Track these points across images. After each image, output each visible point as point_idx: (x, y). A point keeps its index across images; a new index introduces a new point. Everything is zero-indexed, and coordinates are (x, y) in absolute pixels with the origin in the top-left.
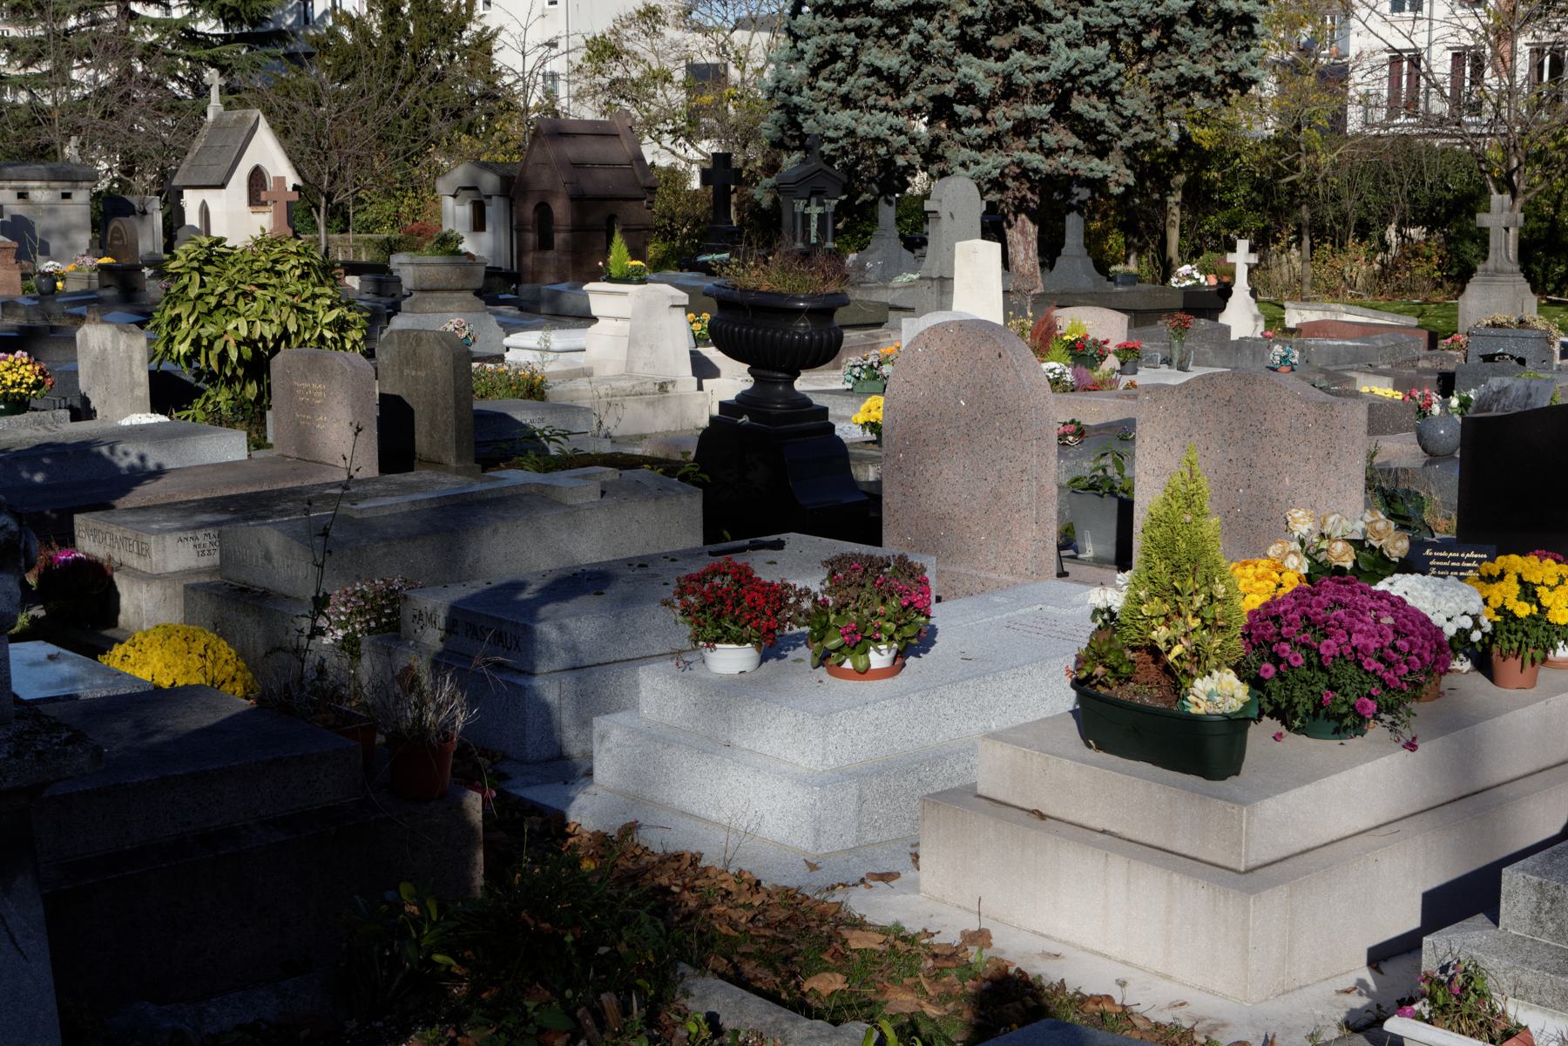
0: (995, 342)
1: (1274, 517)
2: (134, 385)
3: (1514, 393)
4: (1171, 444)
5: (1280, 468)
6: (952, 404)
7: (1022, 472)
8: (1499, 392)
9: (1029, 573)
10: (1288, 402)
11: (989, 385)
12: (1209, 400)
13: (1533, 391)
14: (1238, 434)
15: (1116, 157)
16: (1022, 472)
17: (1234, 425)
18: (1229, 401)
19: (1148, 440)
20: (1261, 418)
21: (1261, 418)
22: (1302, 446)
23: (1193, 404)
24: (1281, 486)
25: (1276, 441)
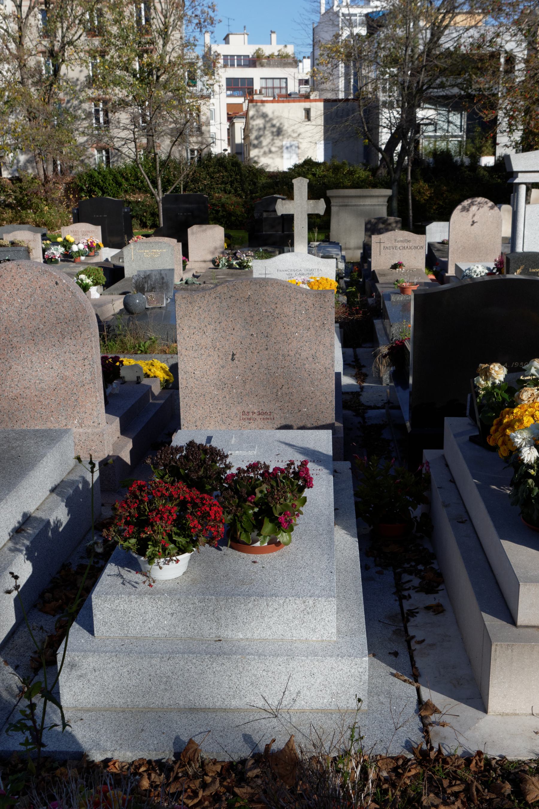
0: (51, 274)
1: (286, 365)
2: (93, 381)
3: (154, 277)
4: (205, 329)
5: (289, 336)
6: (16, 320)
7: (84, 359)
8: (145, 278)
9: (96, 424)
10: (292, 295)
11: (49, 305)
12: (233, 299)
13: (164, 276)
14: (256, 318)
15: (500, 151)
16: (84, 359)
17: (253, 313)
18: (249, 298)
19: (185, 328)
20: (273, 306)
21: (273, 306)
22: (304, 321)
23: (221, 303)
24: (290, 346)
25: (285, 320)
